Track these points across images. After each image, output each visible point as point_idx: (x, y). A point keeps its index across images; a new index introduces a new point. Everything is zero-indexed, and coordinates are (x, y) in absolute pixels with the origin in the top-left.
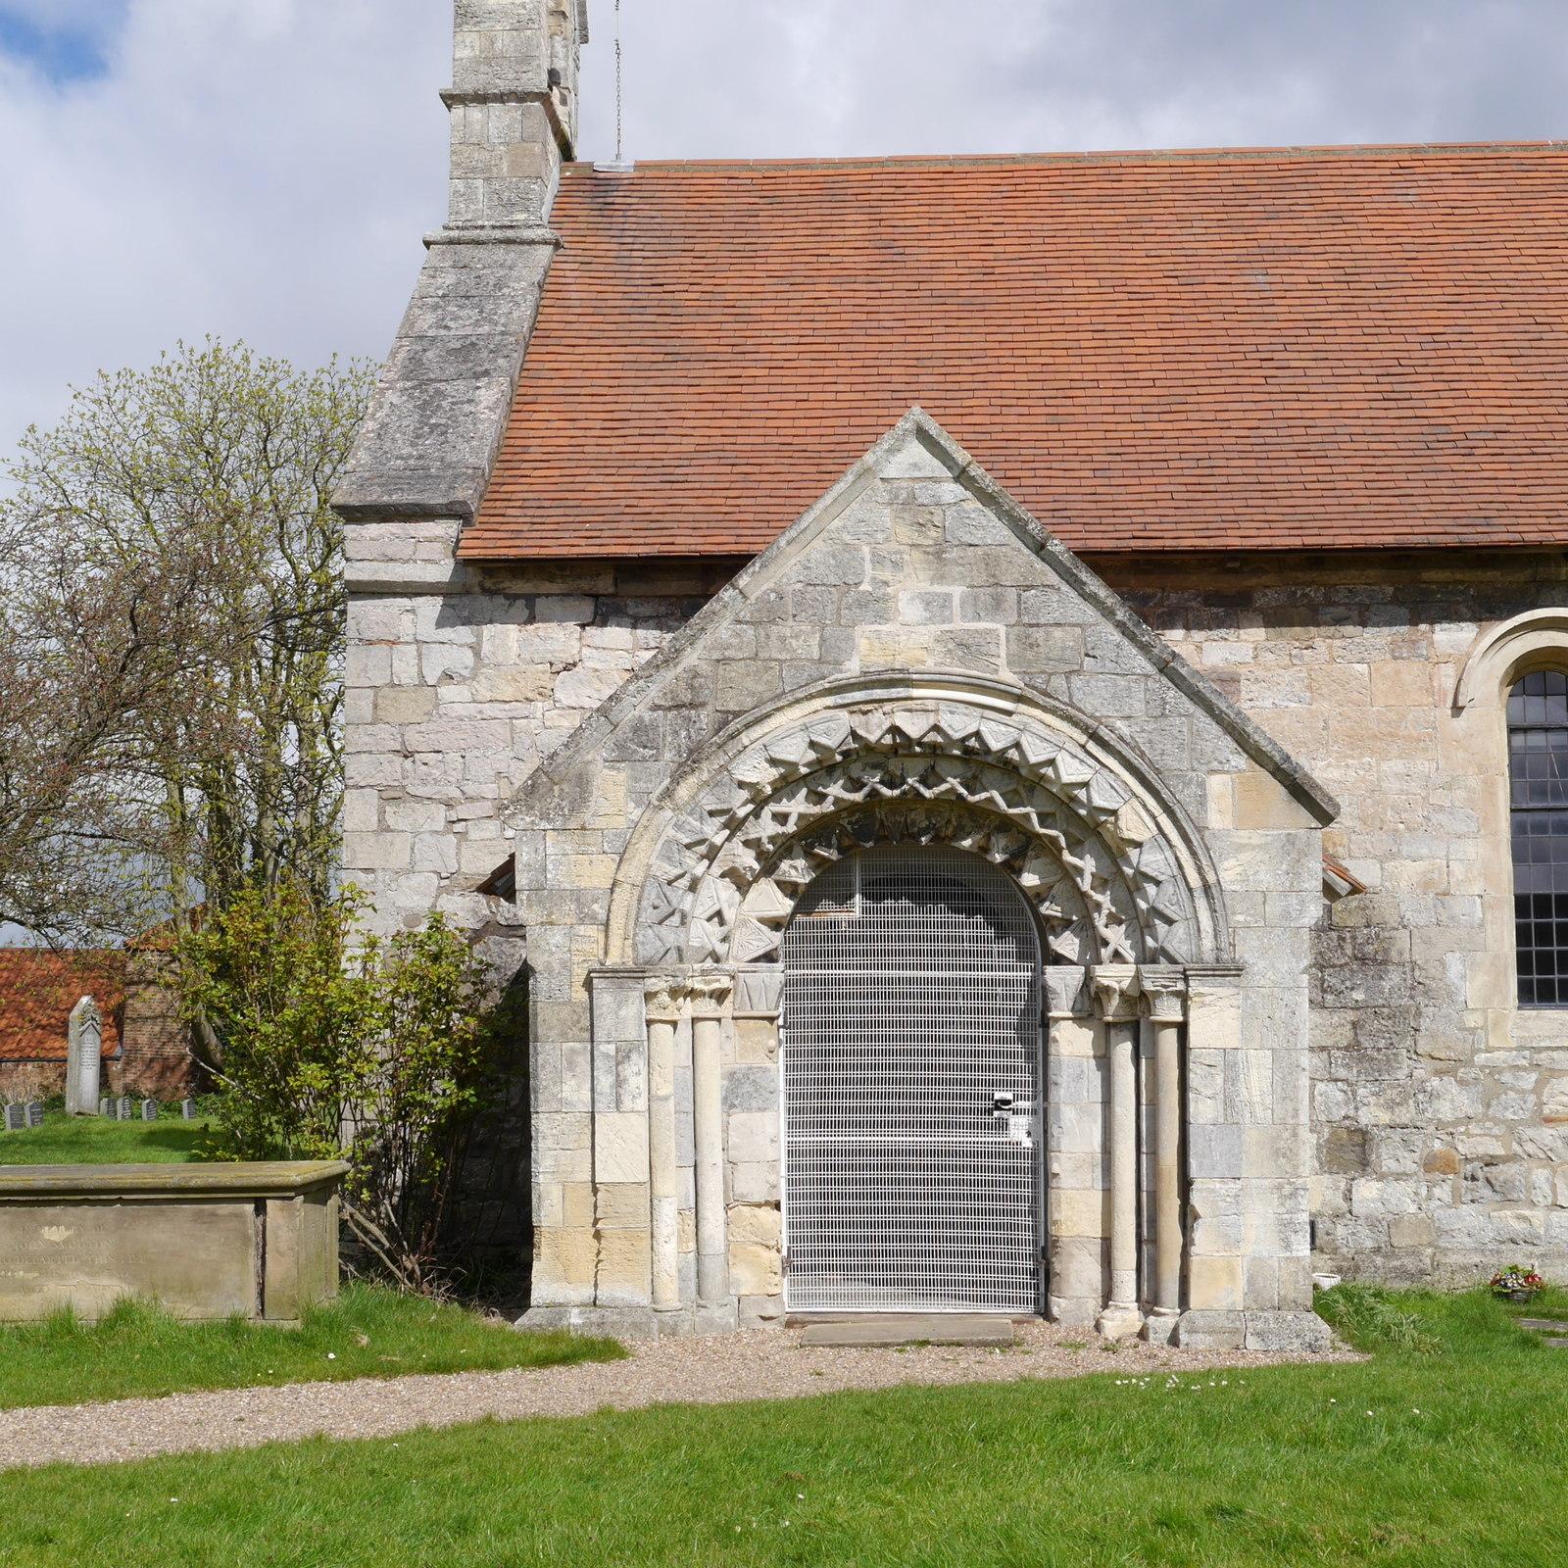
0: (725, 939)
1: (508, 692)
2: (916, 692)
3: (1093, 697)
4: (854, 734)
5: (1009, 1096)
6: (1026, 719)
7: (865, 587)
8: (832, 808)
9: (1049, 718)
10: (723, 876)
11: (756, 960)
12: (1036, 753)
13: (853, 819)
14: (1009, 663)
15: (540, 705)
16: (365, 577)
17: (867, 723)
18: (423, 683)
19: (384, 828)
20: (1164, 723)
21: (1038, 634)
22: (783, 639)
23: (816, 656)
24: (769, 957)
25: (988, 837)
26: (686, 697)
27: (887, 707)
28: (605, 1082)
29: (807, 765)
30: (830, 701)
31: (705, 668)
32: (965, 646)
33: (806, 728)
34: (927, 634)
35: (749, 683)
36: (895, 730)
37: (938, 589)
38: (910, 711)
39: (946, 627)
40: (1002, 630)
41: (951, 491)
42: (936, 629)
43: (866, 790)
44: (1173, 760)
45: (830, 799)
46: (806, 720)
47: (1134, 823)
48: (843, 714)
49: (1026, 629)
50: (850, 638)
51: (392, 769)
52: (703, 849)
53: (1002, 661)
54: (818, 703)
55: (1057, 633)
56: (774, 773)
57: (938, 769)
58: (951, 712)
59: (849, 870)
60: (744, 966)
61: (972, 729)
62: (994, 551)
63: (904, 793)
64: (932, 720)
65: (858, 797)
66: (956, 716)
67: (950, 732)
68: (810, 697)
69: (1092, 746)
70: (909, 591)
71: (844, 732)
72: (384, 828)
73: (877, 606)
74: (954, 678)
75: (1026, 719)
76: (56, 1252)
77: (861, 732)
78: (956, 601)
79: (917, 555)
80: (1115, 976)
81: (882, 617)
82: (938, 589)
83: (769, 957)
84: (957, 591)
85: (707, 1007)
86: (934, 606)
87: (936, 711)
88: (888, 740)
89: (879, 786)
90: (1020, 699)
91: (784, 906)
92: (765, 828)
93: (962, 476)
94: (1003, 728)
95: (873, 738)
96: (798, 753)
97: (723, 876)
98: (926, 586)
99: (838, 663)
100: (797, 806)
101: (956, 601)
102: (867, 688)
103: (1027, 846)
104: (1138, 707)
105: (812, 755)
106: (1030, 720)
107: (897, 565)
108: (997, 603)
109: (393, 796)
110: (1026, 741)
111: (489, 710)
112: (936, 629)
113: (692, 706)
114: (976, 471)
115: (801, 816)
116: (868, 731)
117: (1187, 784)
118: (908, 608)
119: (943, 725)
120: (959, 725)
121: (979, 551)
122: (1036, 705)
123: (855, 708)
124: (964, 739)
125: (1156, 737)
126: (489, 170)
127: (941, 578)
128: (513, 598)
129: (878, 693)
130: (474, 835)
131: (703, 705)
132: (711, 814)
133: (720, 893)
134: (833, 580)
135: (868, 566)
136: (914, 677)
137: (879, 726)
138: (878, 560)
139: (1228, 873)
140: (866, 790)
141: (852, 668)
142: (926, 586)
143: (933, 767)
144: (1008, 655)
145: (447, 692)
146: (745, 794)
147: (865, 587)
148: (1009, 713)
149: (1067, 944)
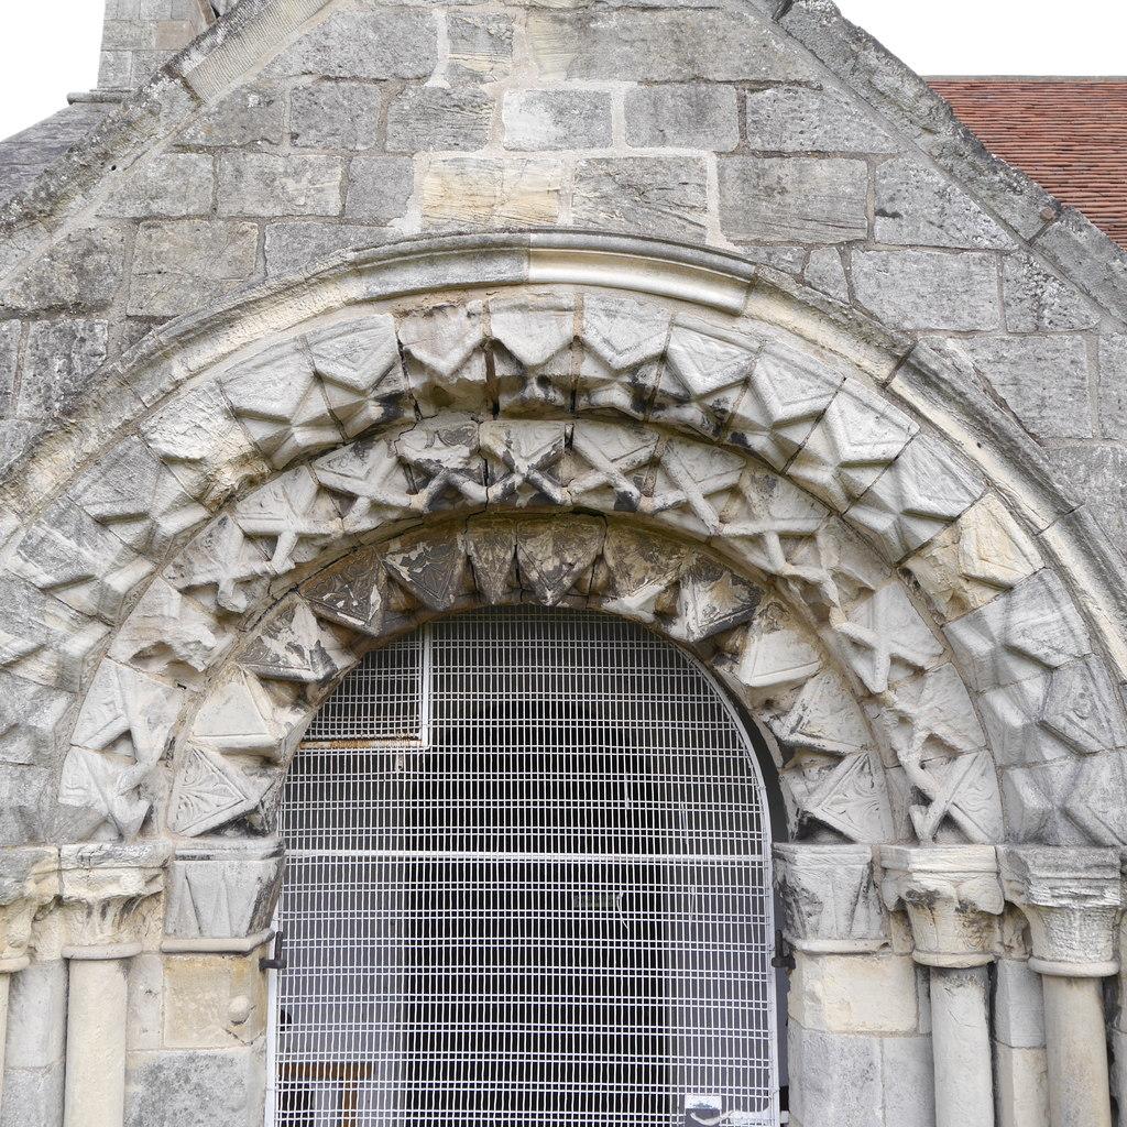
0: (138, 789)
2: (535, 271)
3: (899, 290)
4: (406, 358)
5: (714, 1102)
6: (764, 329)
7: (437, 81)
8: (367, 524)
9: (811, 326)
10: (141, 658)
11: (217, 831)
12: (785, 396)
13: (413, 555)
14: (725, 224)
17: (433, 336)
20: (1041, 345)
21: (785, 170)
22: (268, 179)
23: (333, 205)
24: (244, 824)
25: (675, 586)
26: (69, 290)
27: (476, 302)
29: (316, 423)
30: (356, 288)
31: (110, 234)
33: (305, 346)
34: (559, 167)
35: (197, 264)
36: (493, 348)
37: (579, 85)
38: (523, 308)
39: (598, 153)
40: (711, 163)
42: (578, 157)
43: (434, 484)
45: (362, 504)
46: (306, 329)
47: (993, 542)
48: (384, 319)
49: (757, 159)
50: (404, 175)
52: (82, 596)
53: (711, 219)
54: (333, 295)
55: (821, 169)
56: (239, 440)
57: (579, 442)
58: (610, 314)
59: (412, 659)
60: (184, 846)
61: (653, 348)
62: (693, 18)
63: (510, 492)
64: (568, 327)
65: (419, 501)
66: (620, 324)
67: (607, 353)
68: (321, 280)
69: (899, 384)
70: (524, 93)
71: (384, 355)
73: (461, 117)
74: (615, 241)
75: (764, 329)
77: (419, 353)
78: (617, 108)
79: (539, 24)
81: (468, 136)
82: (579, 85)
83: (244, 824)
84: (620, 90)
85: (98, 936)
86: (575, 117)
87: (578, 310)
88: (477, 372)
89: (459, 478)
90: (752, 285)
91: (276, 723)
92: (229, 561)
94: (716, 346)
95: (444, 364)
96: (281, 392)
97: (141, 658)
99: (378, 222)
100: (289, 511)
101: (617, 108)
102: (432, 261)
103: (764, 594)
104: (988, 312)
105: (318, 405)
106: (771, 332)
107: (501, 43)
108: (699, 116)
110: (763, 373)
112: (578, 157)
113: (79, 308)
115: (303, 539)
116: (435, 352)
117: (1096, 466)
118: (519, 117)
119: (591, 337)
120: (625, 336)
121: (663, 18)
122: (786, 297)
123: (409, 304)
124: (634, 369)
125: (1026, 373)
126: (139, 44)
127: (588, 67)
129: (458, 272)
131: (102, 306)
132: (103, 522)
133: (128, 696)
134: (372, 69)
135: (443, 44)
136: (533, 237)
137: (459, 341)
138: (462, 33)
140: (434, 484)
141: (408, 225)
142: (555, 80)
143: (569, 441)
144: (722, 207)
146: (181, 482)
147: (437, 81)
148: (731, 313)
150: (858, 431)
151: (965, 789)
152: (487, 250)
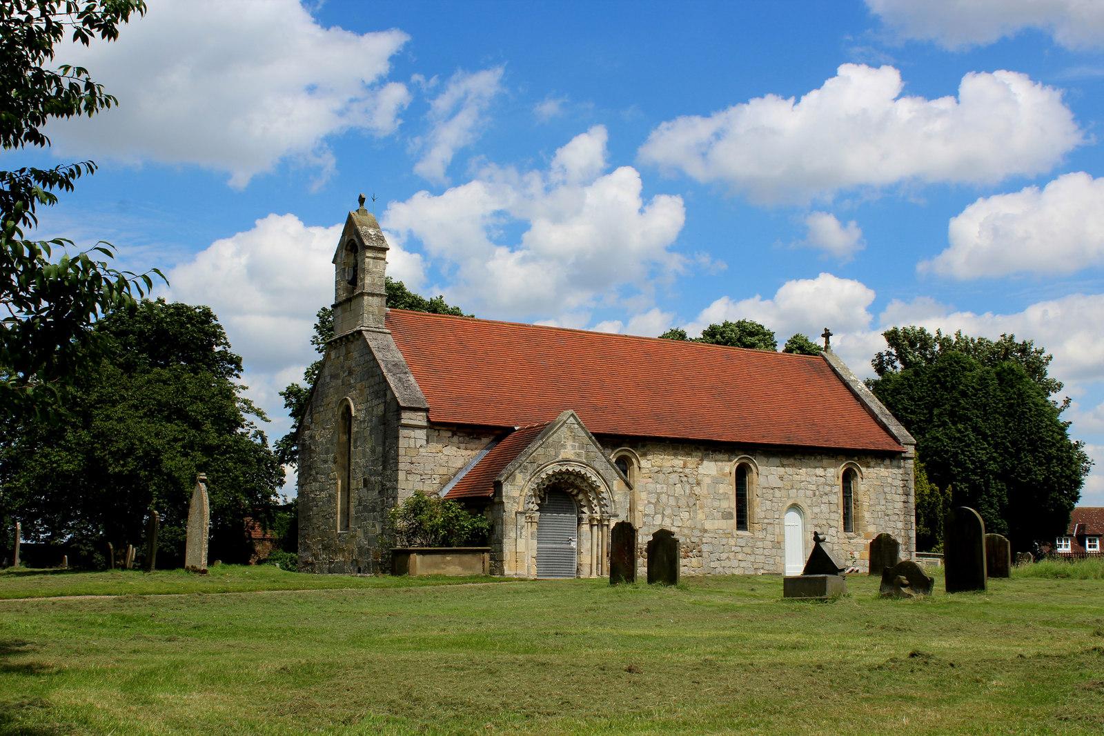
1: (434, 451)
12: (589, 475)
15: (440, 454)
16: (406, 422)
18: (416, 448)
19: (407, 480)
28: (519, 533)
32: (578, 455)
36: (567, 469)
41: (576, 426)
44: (607, 477)
47: (603, 488)
49: (588, 452)
51: (408, 467)
55: (592, 453)
70: (569, 443)
72: (407, 480)
73: (564, 446)
76: (449, 562)
80: (598, 516)
84: (577, 444)
86: (573, 447)
93: (579, 424)
98: (571, 443)
108: (583, 448)
109: (409, 473)
111: (430, 454)
113: (534, 463)
114: (581, 423)
118: (569, 447)
120: (577, 469)
128: (435, 430)
130: (426, 482)
139: (616, 498)
141: (560, 458)
142: (571, 443)
145: (421, 450)
149: (585, 510)
150: (594, 478)
151: (597, 509)
152: (567, 461)
